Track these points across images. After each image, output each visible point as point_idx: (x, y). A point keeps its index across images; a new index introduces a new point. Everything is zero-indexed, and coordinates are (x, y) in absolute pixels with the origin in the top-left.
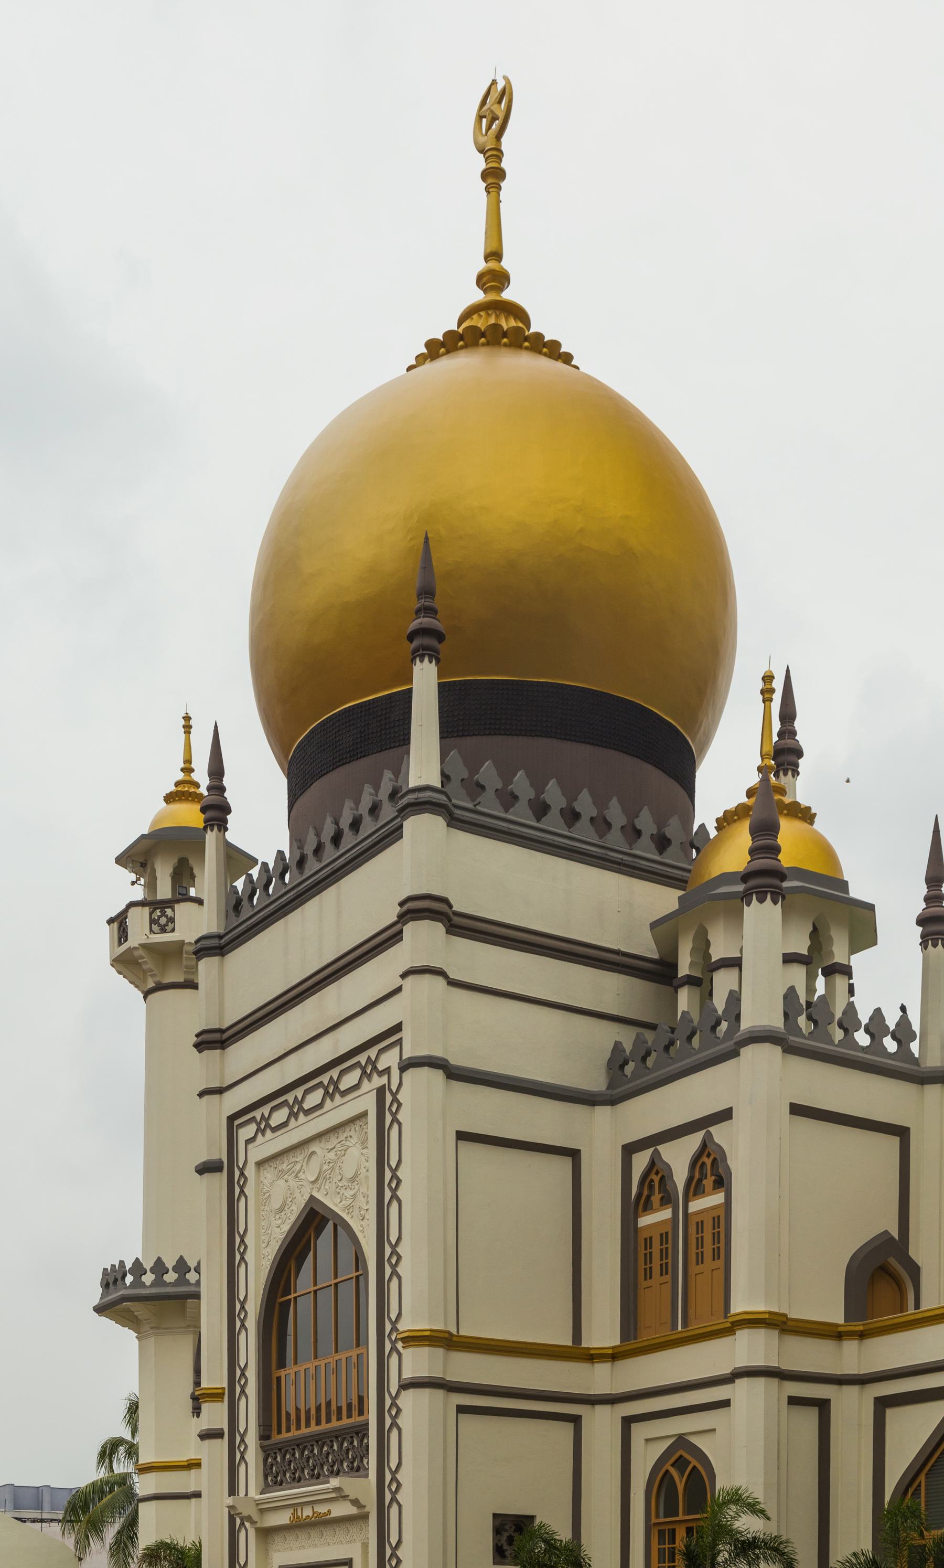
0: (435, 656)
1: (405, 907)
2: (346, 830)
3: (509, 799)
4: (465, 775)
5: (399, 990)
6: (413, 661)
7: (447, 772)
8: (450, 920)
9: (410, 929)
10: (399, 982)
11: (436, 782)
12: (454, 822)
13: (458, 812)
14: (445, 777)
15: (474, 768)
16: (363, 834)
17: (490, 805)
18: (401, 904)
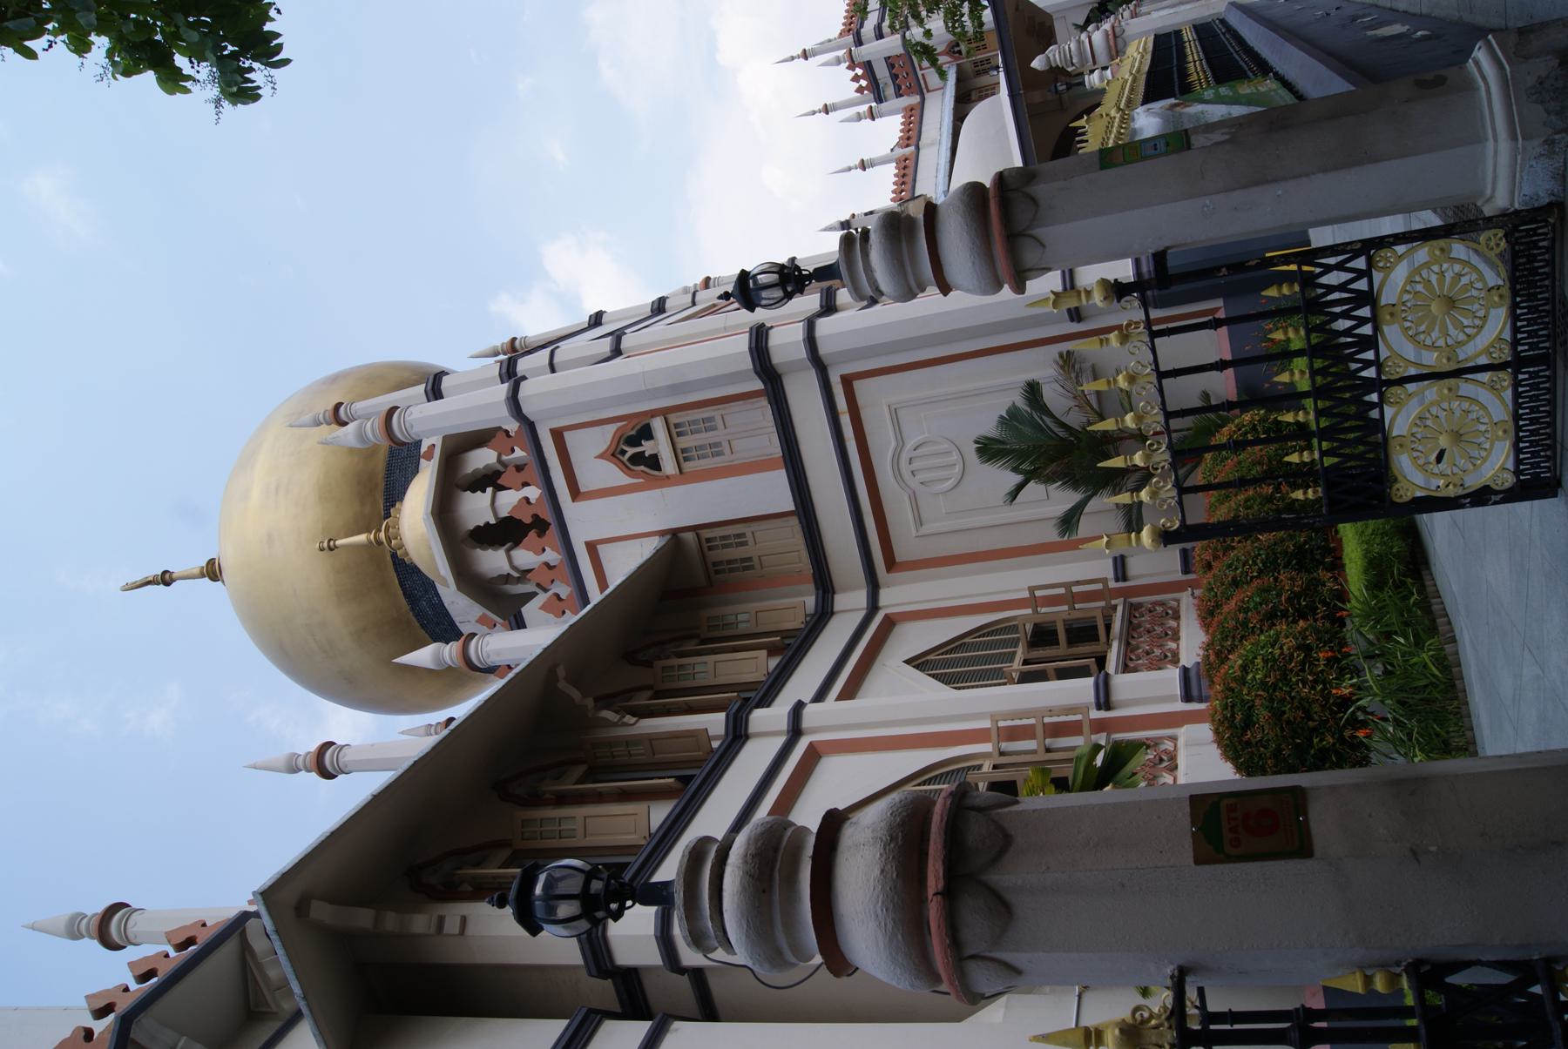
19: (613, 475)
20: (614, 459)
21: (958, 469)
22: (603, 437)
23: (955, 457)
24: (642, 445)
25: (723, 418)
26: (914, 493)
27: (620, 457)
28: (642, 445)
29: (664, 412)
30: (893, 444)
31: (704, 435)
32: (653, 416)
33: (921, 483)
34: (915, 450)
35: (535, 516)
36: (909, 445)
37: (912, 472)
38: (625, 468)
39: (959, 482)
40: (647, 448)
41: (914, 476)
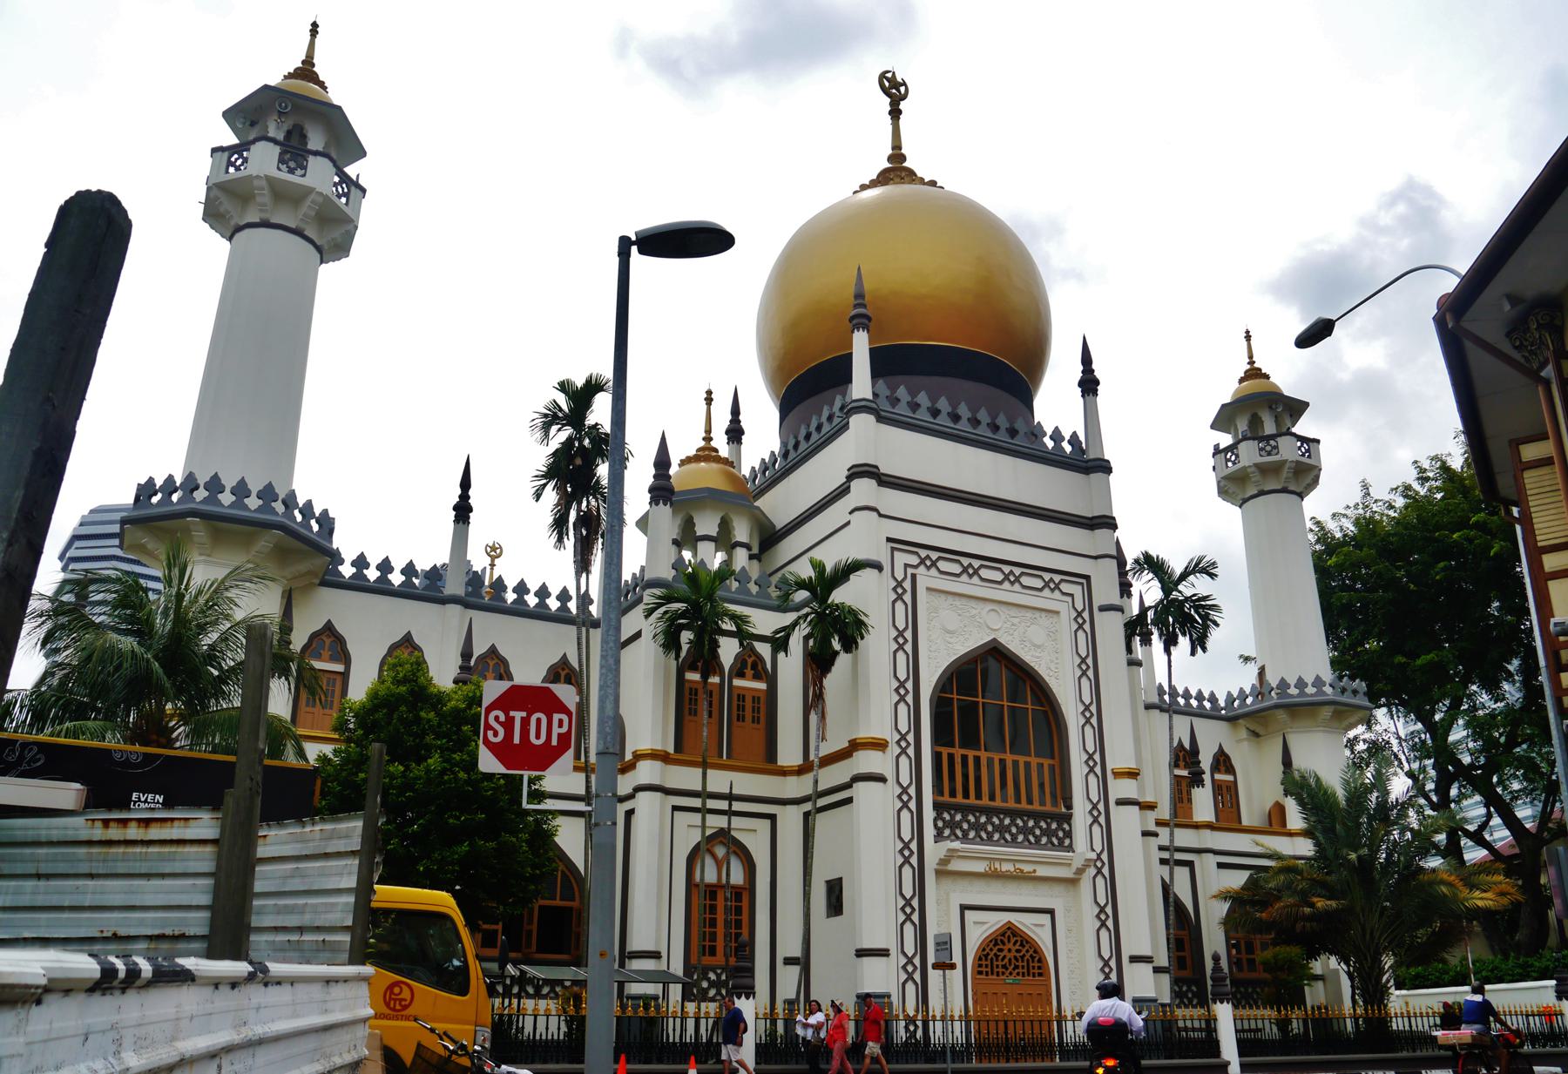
0: (866, 327)
1: (851, 471)
2: (814, 432)
3: (915, 406)
4: (888, 393)
5: (848, 523)
6: (853, 332)
7: (876, 392)
8: (880, 478)
9: (857, 485)
10: (849, 517)
11: (871, 397)
12: (881, 419)
13: (883, 413)
14: (875, 395)
15: (893, 389)
16: (824, 431)
17: (902, 409)
18: (849, 470)
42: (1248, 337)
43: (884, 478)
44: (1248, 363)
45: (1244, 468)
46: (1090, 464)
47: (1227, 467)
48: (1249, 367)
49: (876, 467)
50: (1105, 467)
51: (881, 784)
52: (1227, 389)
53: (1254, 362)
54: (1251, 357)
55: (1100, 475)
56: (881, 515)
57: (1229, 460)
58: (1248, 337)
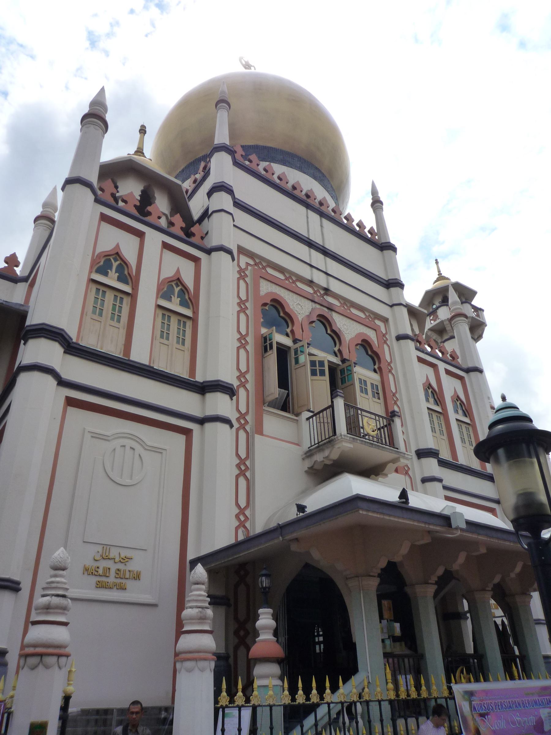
19: (168, 273)
20: (175, 278)
21: (118, 480)
22: (189, 281)
23: (128, 482)
24: (178, 298)
25: (183, 351)
26: (108, 441)
27: (175, 282)
28: (178, 298)
29: (194, 320)
30: (149, 443)
31: (176, 335)
32: (194, 312)
33: (114, 449)
34: (139, 455)
35: (149, 214)
36: (144, 454)
37: (124, 446)
38: (169, 281)
39: (109, 476)
40: (176, 300)
41: (121, 446)
42: (437, 262)
43: (236, 200)
44: (438, 275)
45: (442, 322)
46: (383, 245)
47: (431, 323)
48: (438, 276)
49: (231, 186)
50: (393, 248)
51: (227, 426)
52: (430, 286)
53: (441, 274)
54: (439, 271)
55: (391, 252)
56: (234, 226)
57: (431, 320)
58: (437, 262)
